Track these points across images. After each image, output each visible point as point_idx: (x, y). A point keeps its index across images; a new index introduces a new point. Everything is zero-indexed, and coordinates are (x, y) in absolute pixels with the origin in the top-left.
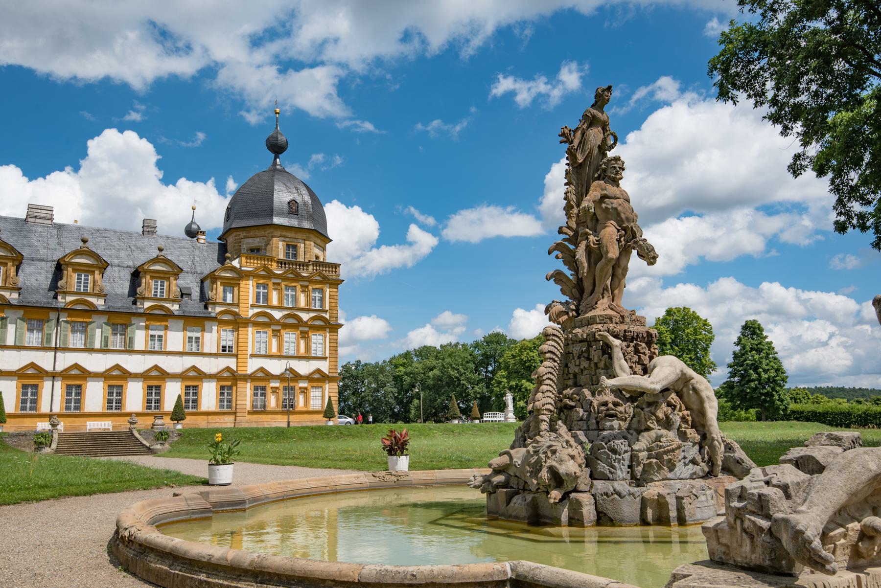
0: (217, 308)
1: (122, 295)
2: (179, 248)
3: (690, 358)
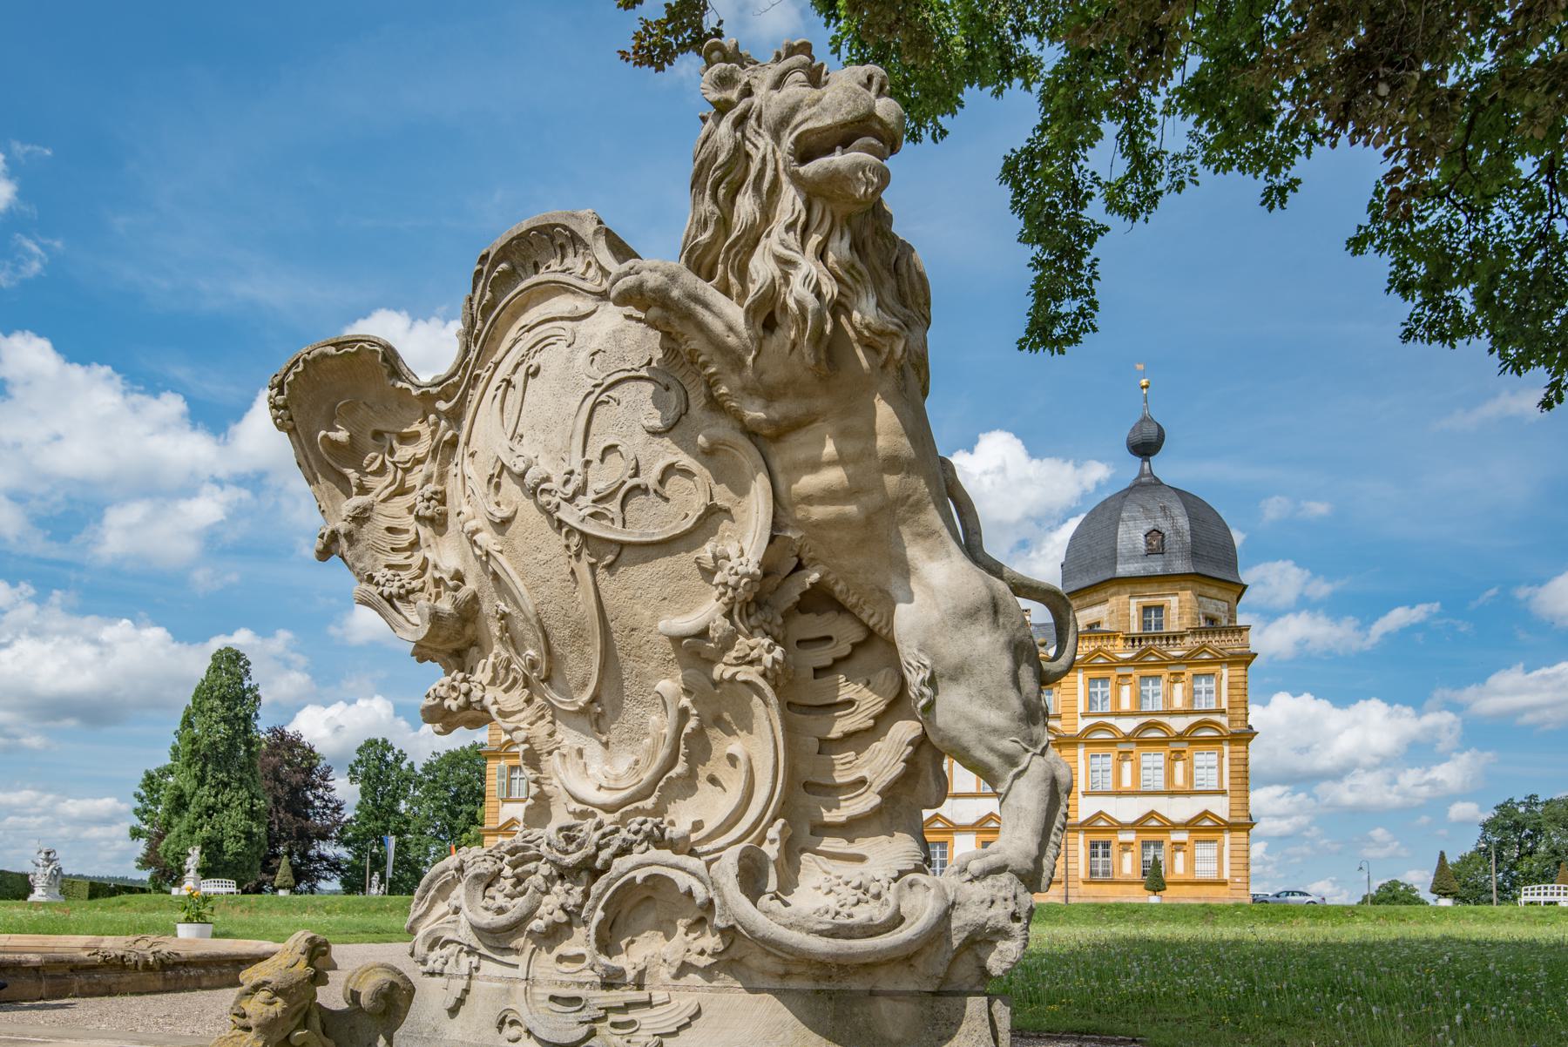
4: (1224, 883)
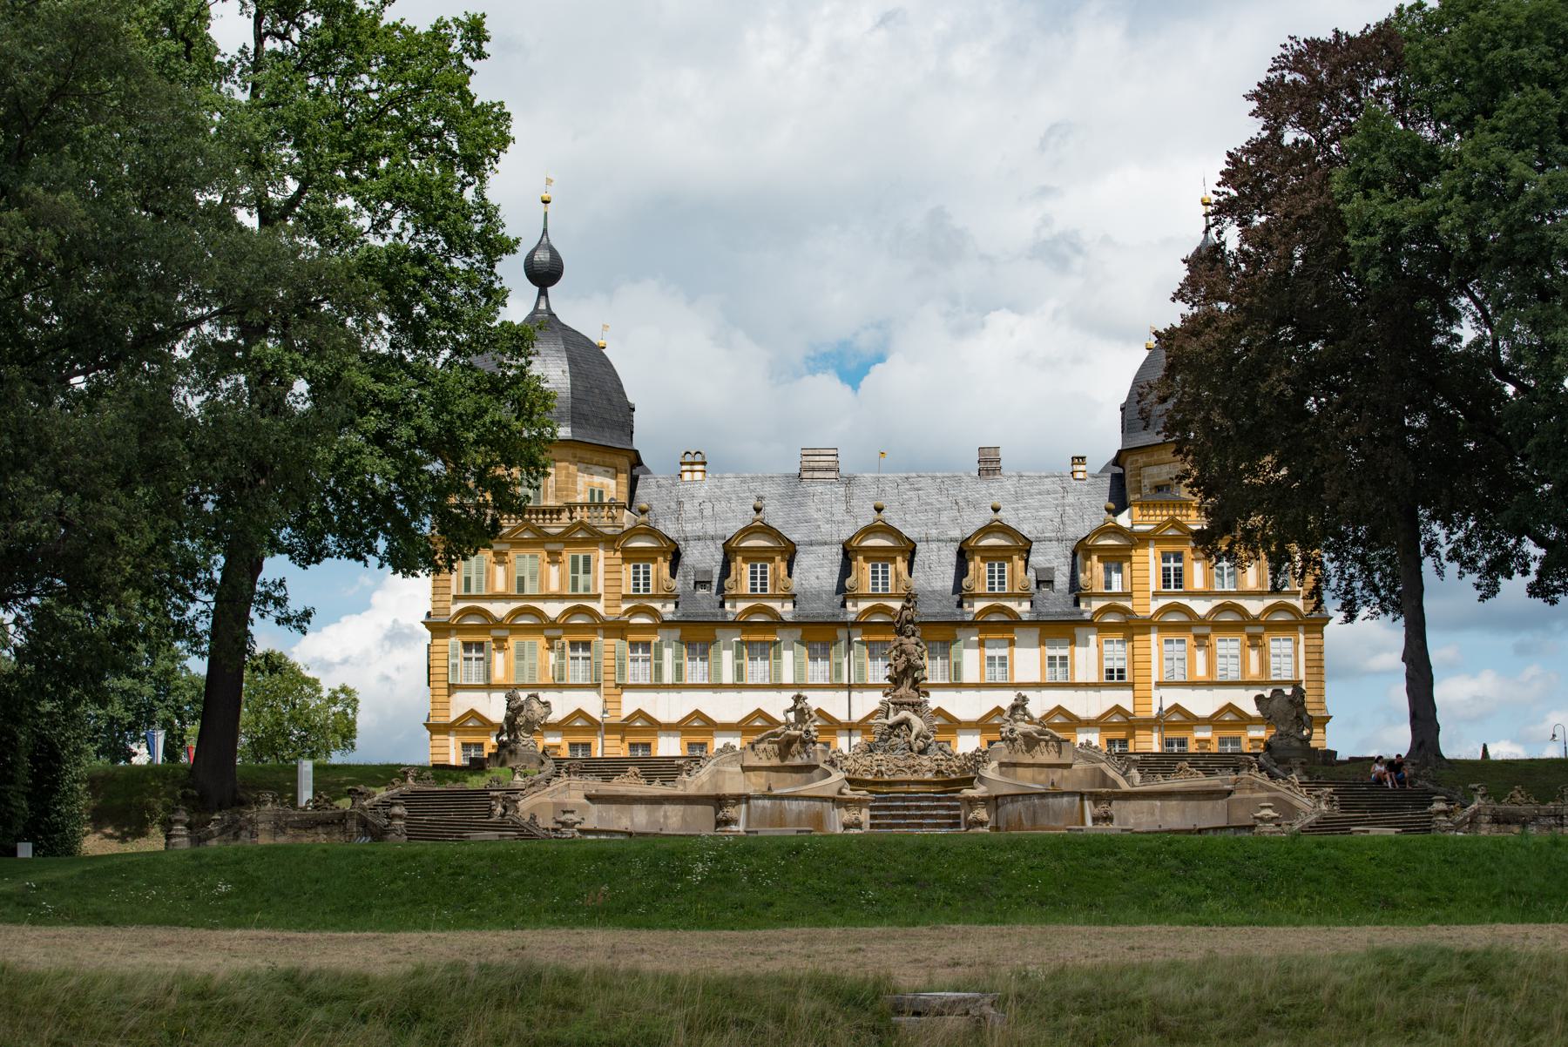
0: (1093, 603)
1: (941, 593)
2: (1040, 494)
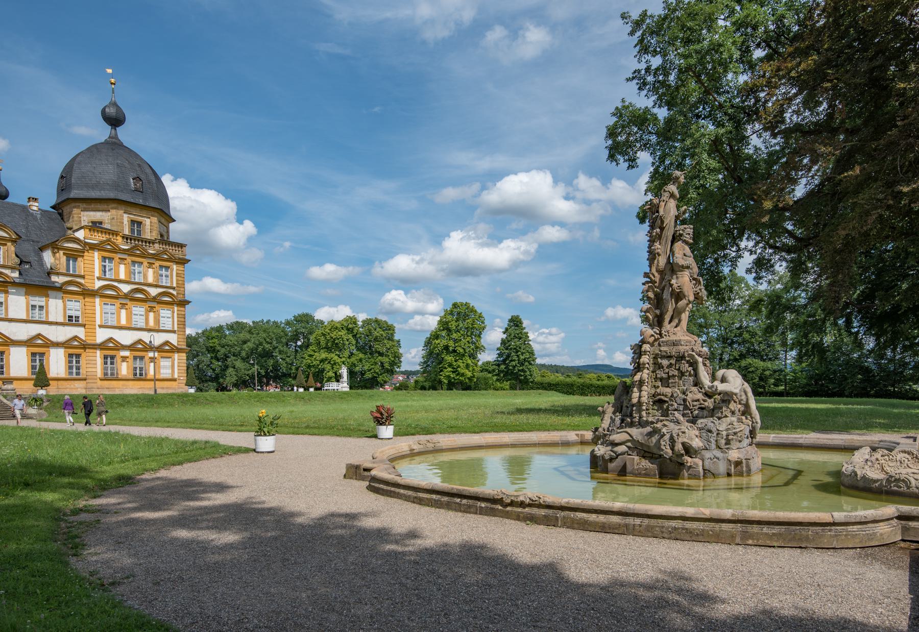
3: (468, 342)
4: (175, 380)
